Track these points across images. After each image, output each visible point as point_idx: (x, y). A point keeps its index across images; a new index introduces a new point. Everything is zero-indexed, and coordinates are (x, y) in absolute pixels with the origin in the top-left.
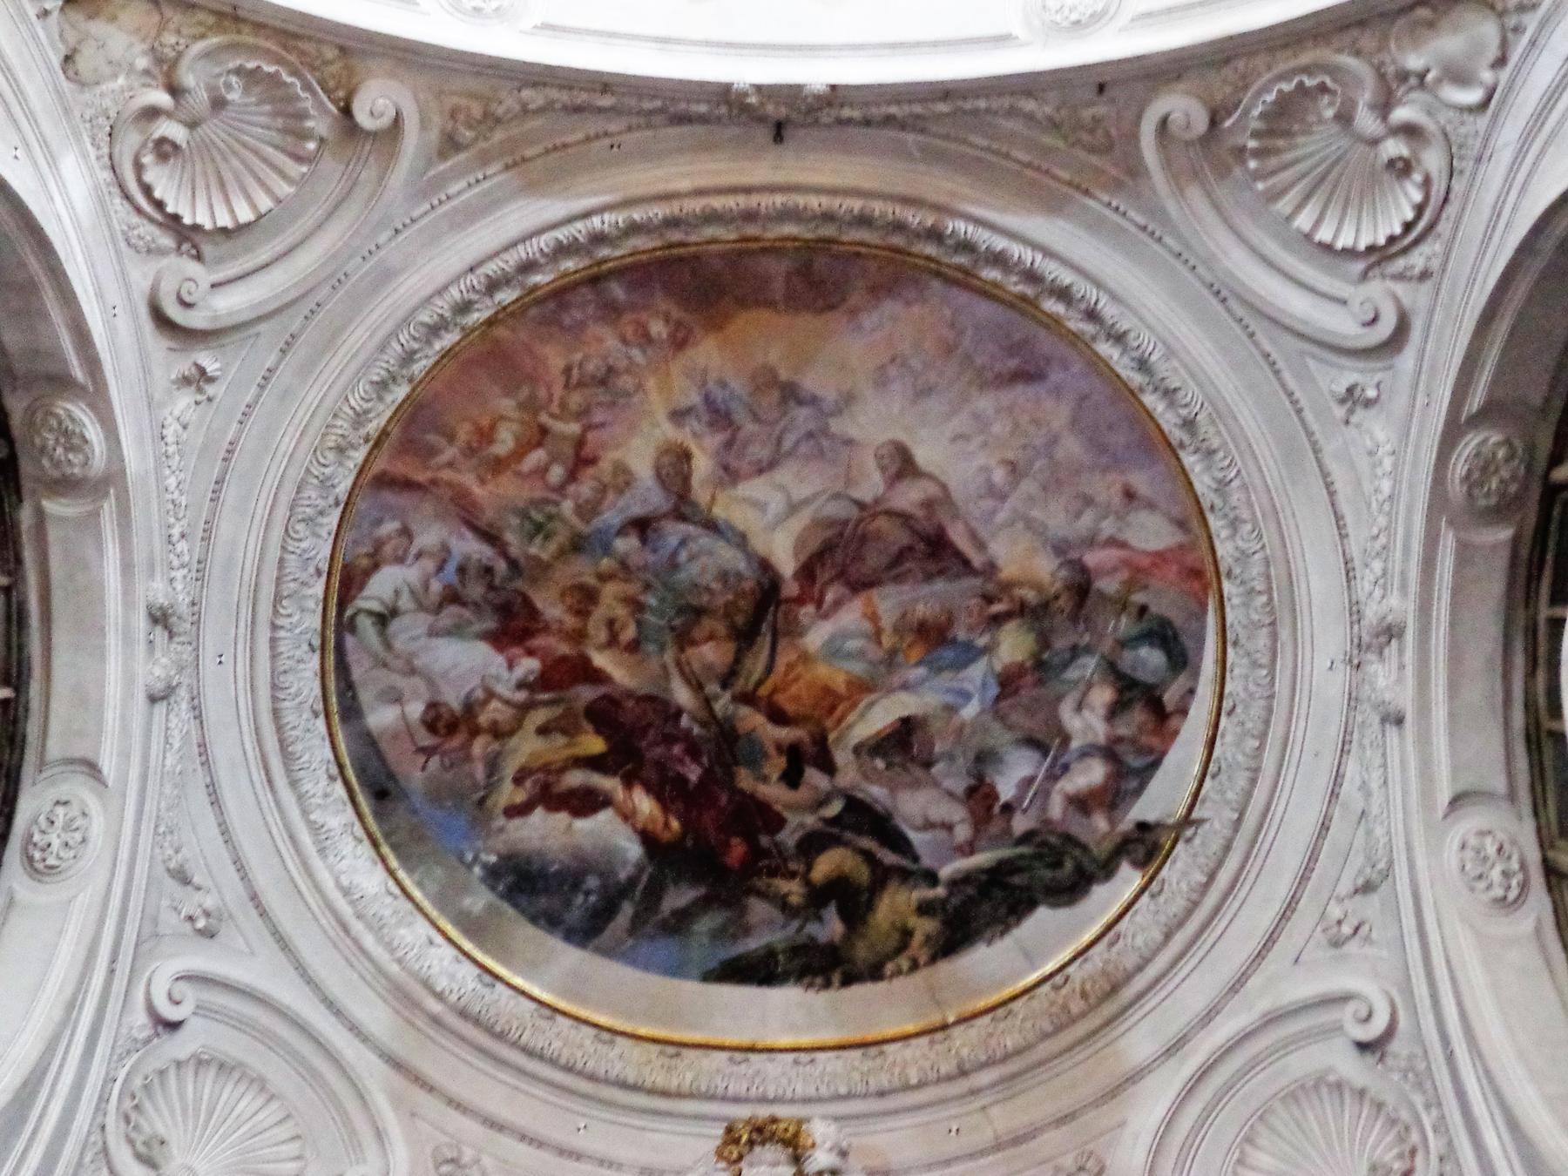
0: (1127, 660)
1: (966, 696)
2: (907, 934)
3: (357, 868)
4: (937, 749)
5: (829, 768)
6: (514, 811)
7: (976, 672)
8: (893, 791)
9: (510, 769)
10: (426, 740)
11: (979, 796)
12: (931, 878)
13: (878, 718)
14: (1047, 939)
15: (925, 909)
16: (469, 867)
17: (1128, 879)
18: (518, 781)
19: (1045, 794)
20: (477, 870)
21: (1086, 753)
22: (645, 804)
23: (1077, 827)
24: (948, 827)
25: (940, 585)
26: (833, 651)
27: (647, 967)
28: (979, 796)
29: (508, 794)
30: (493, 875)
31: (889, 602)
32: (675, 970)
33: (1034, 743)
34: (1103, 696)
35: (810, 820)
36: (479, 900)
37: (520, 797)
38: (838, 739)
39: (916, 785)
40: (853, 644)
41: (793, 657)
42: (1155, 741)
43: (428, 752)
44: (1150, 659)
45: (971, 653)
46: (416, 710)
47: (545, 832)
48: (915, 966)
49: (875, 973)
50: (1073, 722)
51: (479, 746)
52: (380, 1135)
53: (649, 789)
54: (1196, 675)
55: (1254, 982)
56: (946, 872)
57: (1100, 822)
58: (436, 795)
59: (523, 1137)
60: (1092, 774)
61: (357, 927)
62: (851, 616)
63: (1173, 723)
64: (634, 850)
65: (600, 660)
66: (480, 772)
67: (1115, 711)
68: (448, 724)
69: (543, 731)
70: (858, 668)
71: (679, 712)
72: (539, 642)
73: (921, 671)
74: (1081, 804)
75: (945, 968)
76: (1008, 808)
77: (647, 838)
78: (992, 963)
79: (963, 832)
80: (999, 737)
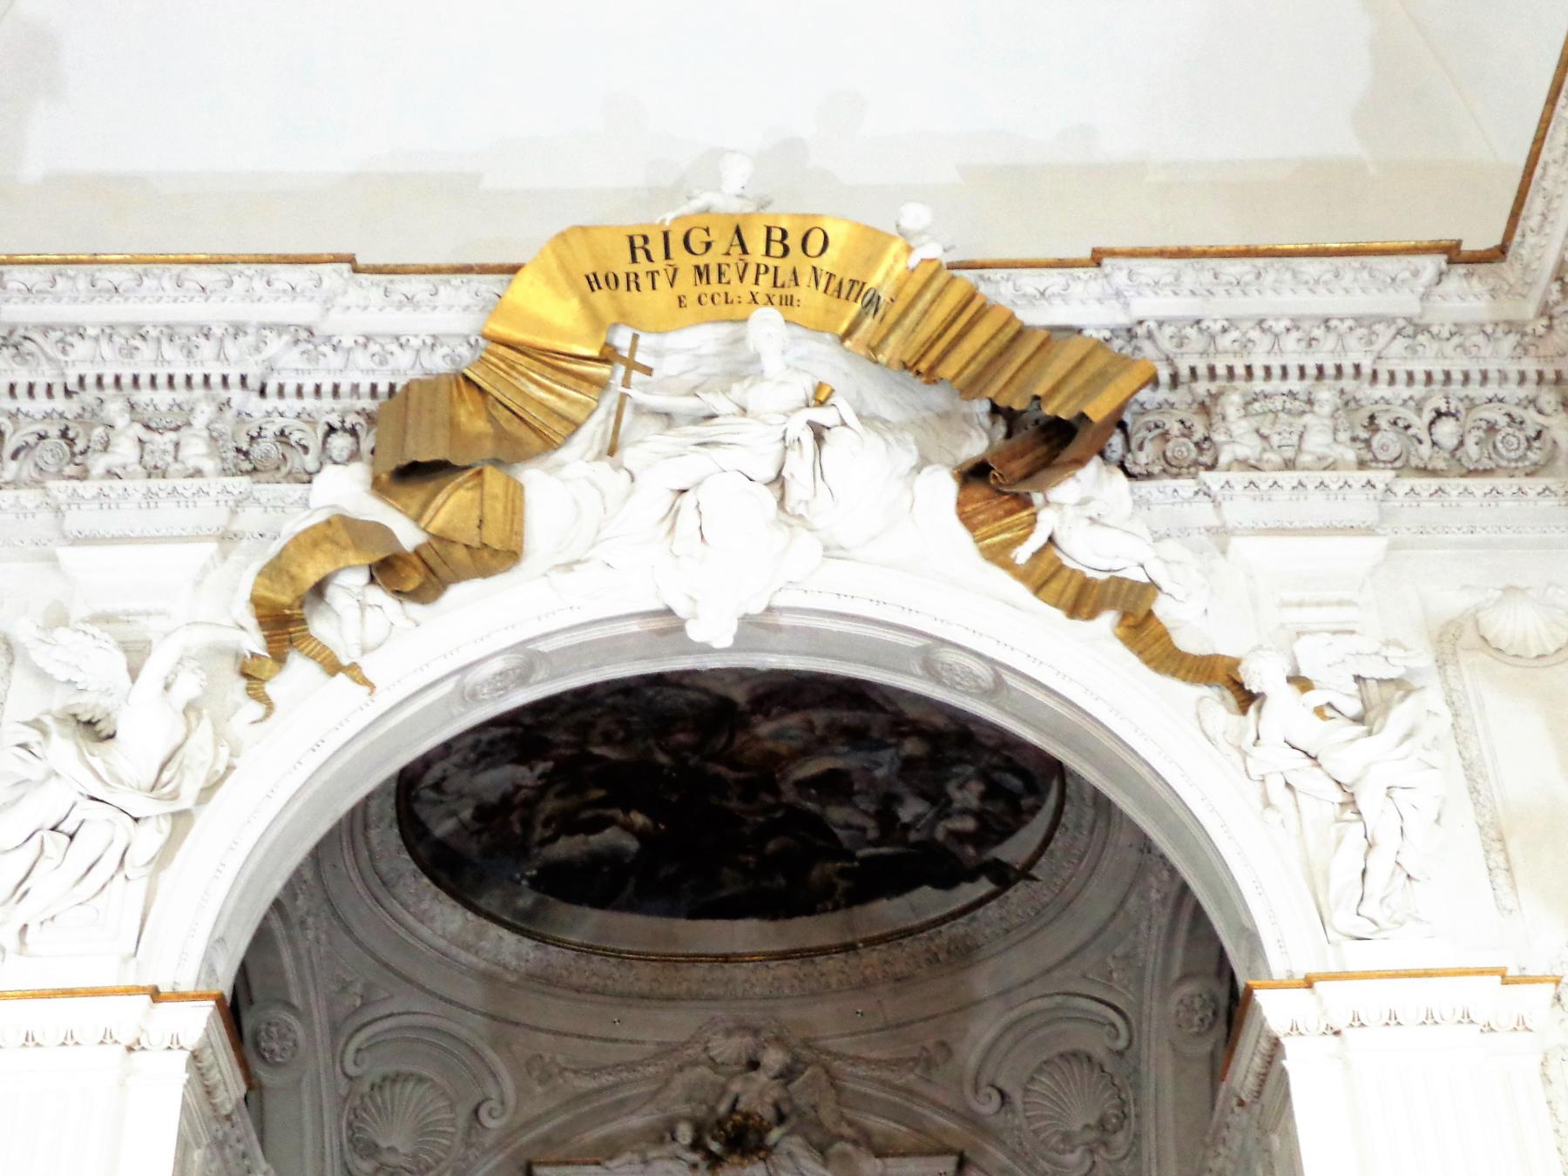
0: (996, 775)
1: (880, 765)
2: (833, 887)
3: (446, 919)
4: (856, 787)
5: (777, 793)
6: (544, 842)
7: (886, 755)
8: (823, 807)
9: (541, 817)
10: (477, 826)
11: (886, 815)
12: (850, 856)
13: (813, 768)
14: (927, 901)
15: (843, 873)
16: (518, 883)
17: (984, 886)
18: (546, 824)
19: (932, 825)
20: (524, 882)
21: (965, 812)
22: (639, 819)
23: (955, 849)
24: (863, 830)
25: (860, 713)
26: (777, 736)
27: (648, 913)
28: (886, 815)
29: (539, 833)
30: (535, 883)
31: (820, 717)
32: (671, 913)
33: (923, 795)
34: (976, 787)
35: (761, 819)
36: (526, 900)
37: (548, 833)
38: (784, 778)
39: (841, 804)
40: (792, 733)
41: (744, 738)
42: (1009, 819)
43: (479, 832)
44: (1014, 782)
45: (880, 745)
46: (467, 814)
47: (566, 847)
48: (836, 908)
49: (810, 911)
50: (957, 795)
51: (514, 817)
52: (494, 1075)
53: (641, 811)
54: (1044, 801)
55: (1056, 974)
56: (861, 853)
57: (971, 851)
58: (488, 853)
59: (579, 1036)
60: (969, 824)
61: (454, 950)
62: (793, 720)
63: (1025, 817)
64: (632, 845)
65: (597, 751)
66: (518, 829)
67: (984, 797)
68: (488, 814)
69: (559, 795)
70: (796, 744)
71: (662, 766)
72: (554, 753)
73: (846, 749)
74: (959, 837)
75: (857, 910)
76: (907, 827)
77: (640, 834)
78: (890, 911)
79: (872, 834)
80: (900, 788)
